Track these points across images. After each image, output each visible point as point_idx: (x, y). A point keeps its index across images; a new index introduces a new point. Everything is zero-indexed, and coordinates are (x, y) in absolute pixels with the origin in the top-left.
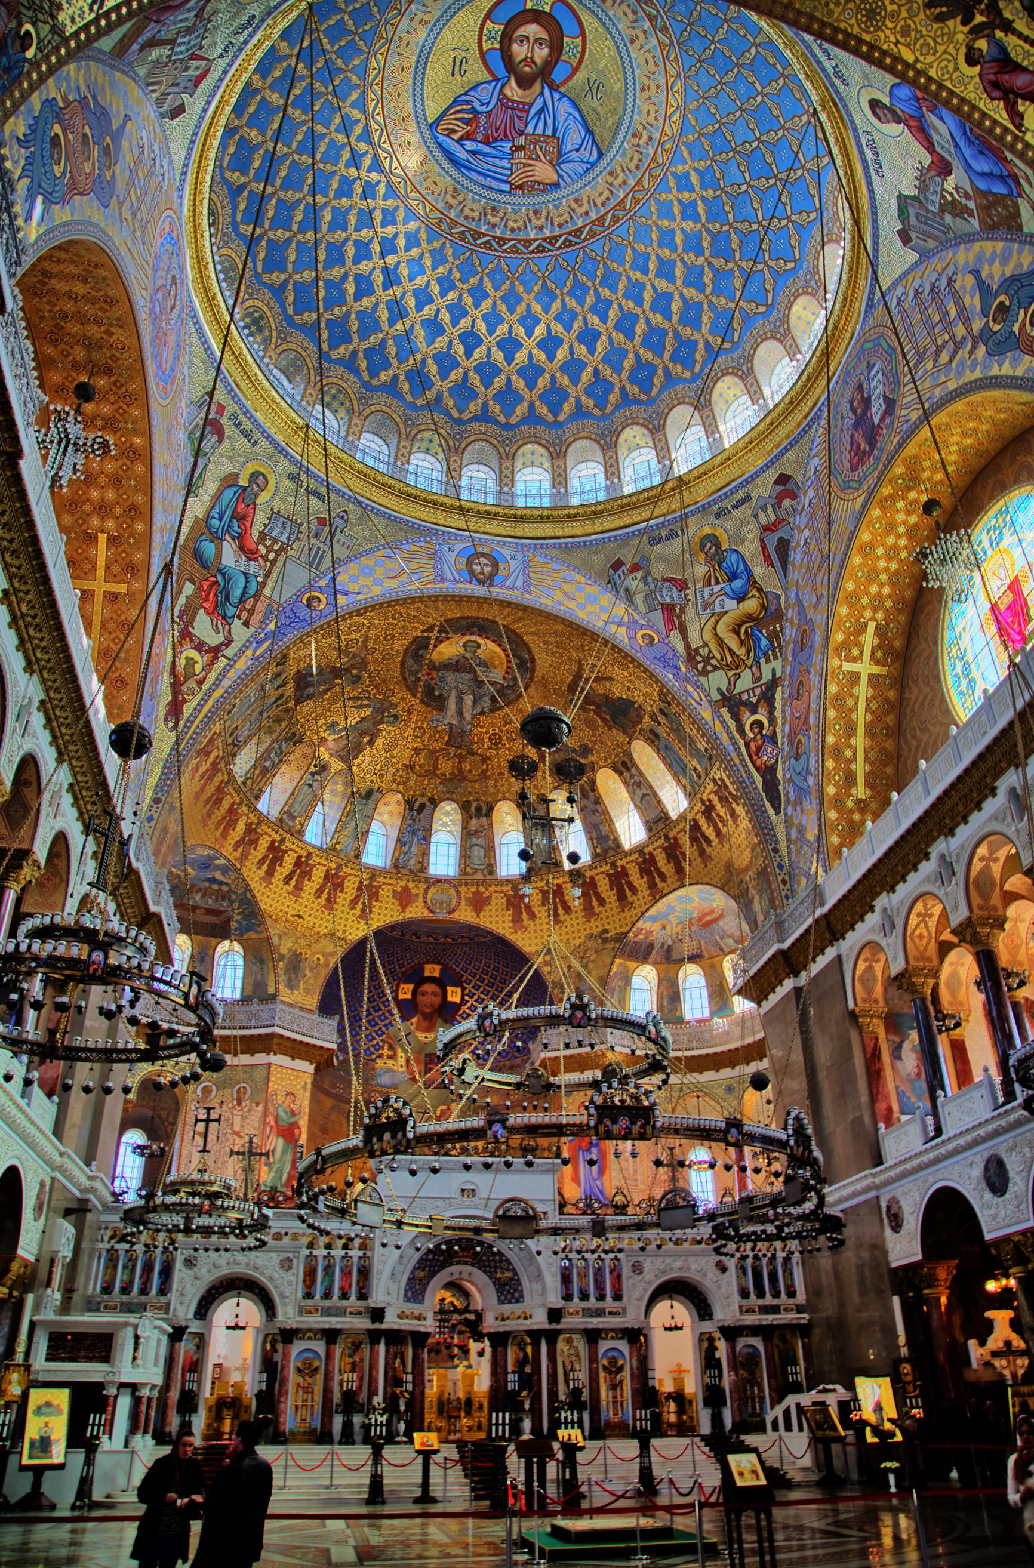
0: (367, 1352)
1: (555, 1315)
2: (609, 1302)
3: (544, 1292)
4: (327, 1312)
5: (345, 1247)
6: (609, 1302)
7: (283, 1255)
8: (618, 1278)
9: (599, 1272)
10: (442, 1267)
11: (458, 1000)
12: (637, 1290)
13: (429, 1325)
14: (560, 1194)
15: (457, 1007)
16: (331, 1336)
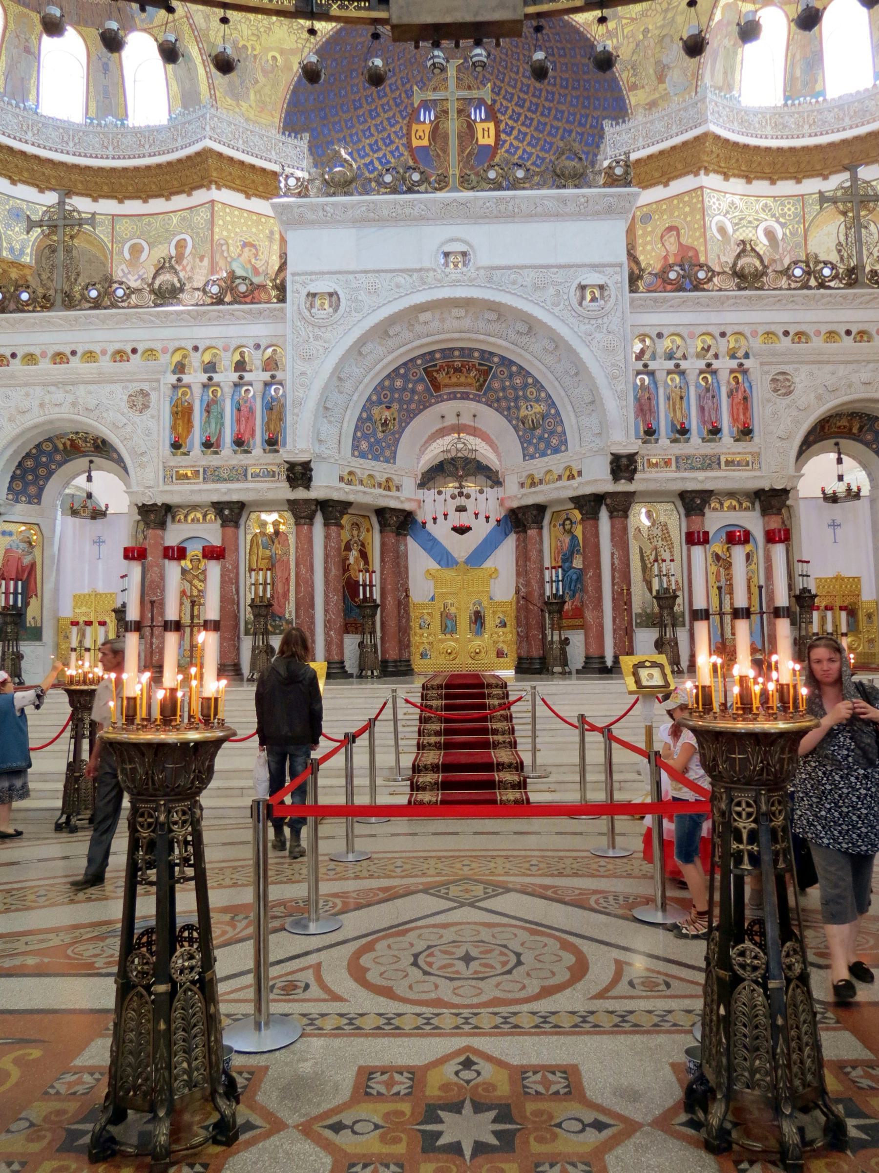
0: (292, 539)
1: (623, 466)
2: (727, 445)
3: (603, 429)
4: (212, 475)
5: (240, 366)
6: (727, 445)
7: (135, 387)
8: (743, 402)
9: (709, 393)
10: (424, 406)
11: (491, 141)
12: (782, 421)
13: (406, 496)
14: (632, 256)
15: (491, 151)
16: (231, 513)
